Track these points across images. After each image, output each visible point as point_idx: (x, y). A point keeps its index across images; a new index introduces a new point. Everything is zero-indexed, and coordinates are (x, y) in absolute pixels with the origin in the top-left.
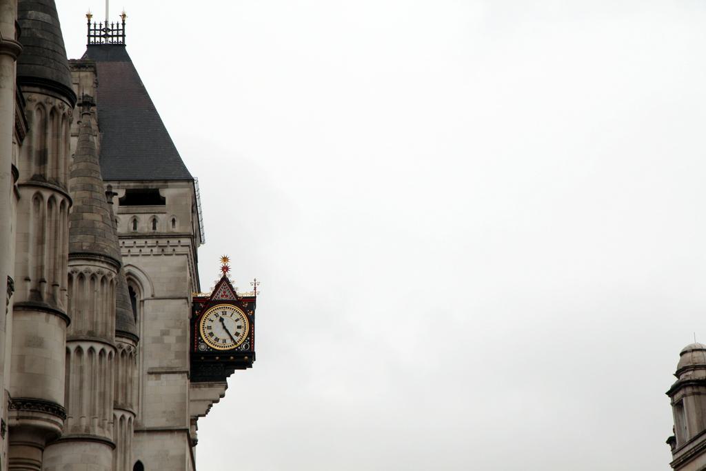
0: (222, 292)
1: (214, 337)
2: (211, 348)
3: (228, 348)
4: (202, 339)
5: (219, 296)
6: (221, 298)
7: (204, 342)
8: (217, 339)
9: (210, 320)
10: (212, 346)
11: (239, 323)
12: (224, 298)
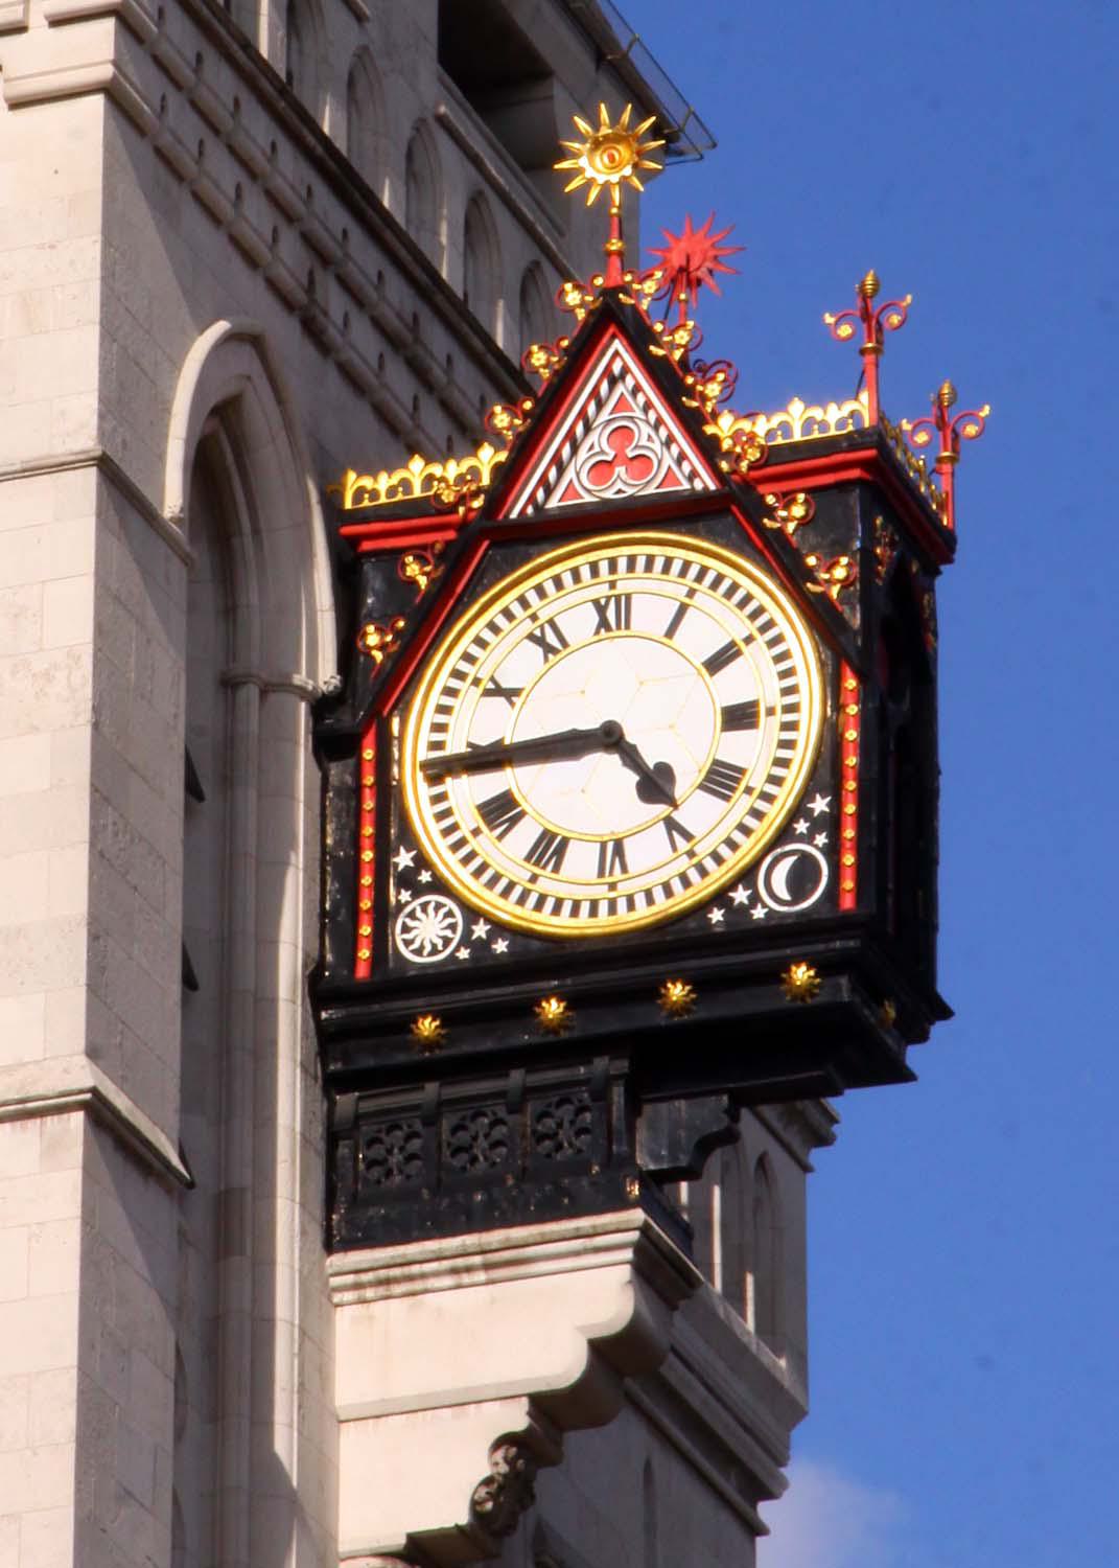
0: (598, 442)
1: (524, 836)
2: (499, 928)
3: (643, 914)
4: (422, 862)
5: (575, 475)
6: (590, 493)
7: (440, 886)
8: (550, 849)
9: (497, 691)
10: (507, 910)
11: (734, 686)
12: (622, 486)
